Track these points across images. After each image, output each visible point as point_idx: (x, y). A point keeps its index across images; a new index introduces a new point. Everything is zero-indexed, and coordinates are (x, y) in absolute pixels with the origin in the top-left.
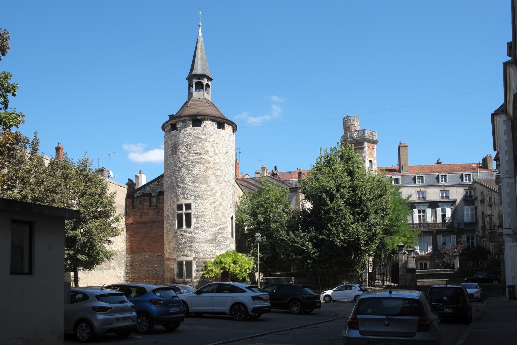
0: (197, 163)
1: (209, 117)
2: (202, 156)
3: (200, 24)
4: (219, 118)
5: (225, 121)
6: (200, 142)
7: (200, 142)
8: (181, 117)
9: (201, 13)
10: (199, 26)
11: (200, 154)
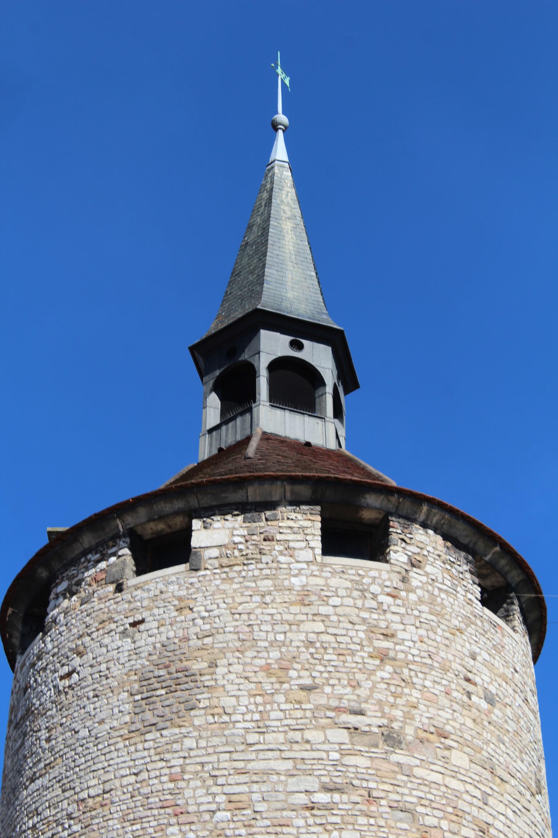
0: (371, 798)
1: (437, 517)
2: (399, 757)
3: (282, 118)
4: (492, 538)
5: (515, 576)
6: (383, 657)
7: (383, 657)
8: (242, 483)
9: (283, 78)
10: (275, 127)
11: (392, 739)
